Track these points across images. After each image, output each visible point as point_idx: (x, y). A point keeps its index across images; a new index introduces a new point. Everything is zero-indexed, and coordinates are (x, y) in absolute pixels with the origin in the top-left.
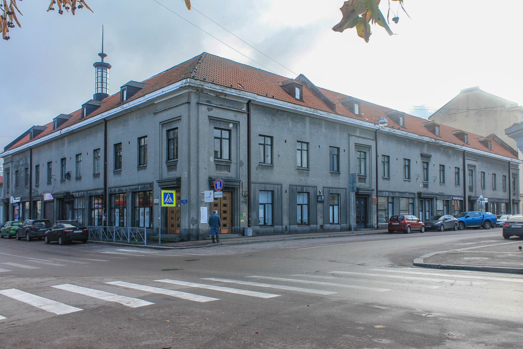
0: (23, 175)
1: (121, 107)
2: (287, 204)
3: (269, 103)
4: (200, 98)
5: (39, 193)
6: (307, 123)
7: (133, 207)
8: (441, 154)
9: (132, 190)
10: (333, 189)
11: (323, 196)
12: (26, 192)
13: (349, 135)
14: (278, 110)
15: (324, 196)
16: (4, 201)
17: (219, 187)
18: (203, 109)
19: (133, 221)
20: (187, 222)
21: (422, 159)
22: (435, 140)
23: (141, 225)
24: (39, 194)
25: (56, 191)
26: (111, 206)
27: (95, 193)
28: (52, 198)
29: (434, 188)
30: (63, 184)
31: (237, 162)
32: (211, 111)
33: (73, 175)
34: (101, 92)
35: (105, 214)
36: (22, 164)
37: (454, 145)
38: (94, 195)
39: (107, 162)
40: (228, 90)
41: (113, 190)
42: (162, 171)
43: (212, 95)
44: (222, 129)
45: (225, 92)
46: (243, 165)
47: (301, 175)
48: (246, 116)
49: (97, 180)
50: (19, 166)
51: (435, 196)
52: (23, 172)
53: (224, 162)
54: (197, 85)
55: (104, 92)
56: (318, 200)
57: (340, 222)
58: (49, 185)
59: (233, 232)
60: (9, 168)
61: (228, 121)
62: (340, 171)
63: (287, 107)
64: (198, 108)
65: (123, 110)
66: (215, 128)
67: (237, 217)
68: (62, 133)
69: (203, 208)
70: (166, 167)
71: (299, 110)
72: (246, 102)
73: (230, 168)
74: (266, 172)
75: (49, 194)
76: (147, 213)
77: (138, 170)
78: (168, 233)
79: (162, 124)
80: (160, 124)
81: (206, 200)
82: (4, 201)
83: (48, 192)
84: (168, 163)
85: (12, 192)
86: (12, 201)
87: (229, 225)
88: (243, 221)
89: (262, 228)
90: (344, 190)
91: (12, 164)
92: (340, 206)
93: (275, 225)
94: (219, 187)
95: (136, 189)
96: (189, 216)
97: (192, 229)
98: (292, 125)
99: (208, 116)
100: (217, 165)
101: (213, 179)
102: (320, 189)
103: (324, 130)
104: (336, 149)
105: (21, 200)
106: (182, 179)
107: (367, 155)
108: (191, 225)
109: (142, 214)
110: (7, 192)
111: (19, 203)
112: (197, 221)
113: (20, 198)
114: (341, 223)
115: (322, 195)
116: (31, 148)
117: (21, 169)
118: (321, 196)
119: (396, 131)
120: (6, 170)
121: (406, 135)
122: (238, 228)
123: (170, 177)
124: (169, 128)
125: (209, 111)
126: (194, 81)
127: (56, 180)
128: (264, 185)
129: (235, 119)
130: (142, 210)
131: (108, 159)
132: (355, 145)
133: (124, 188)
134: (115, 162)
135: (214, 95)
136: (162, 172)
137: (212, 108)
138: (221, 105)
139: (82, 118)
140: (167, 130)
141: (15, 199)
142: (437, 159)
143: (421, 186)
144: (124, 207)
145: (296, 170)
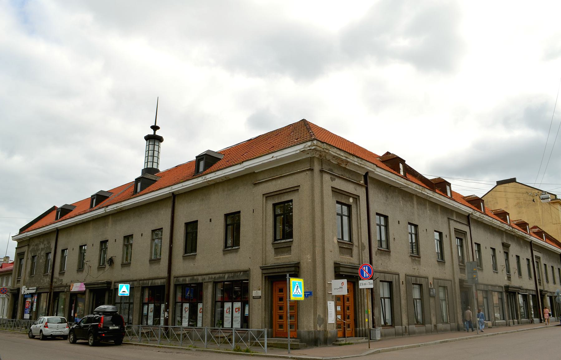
0: (42, 261)
1: (202, 178)
2: (404, 298)
3: (386, 176)
4: (323, 165)
5: (64, 283)
6: (415, 203)
7: (214, 302)
8: (516, 244)
9: (213, 280)
10: (445, 281)
11: (434, 289)
12: (45, 281)
13: (448, 218)
14: (391, 186)
15: (435, 289)
16: (12, 291)
18: (327, 177)
19: (214, 320)
20: (312, 322)
21: (504, 249)
22: (512, 228)
23: (227, 325)
24: (63, 283)
25: (88, 281)
26: (175, 300)
27: (151, 283)
28: (84, 289)
29: (516, 282)
30: (101, 272)
31: (359, 244)
32: (333, 181)
33: (118, 261)
34: (152, 167)
35: (168, 310)
36: (42, 248)
37: (525, 234)
38: (149, 285)
39: (173, 244)
40: (351, 158)
41: (181, 279)
42: (265, 254)
43: (334, 162)
44: (342, 204)
45: (348, 160)
47: (414, 263)
48: (364, 190)
49: (155, 267)
50: (38, 250)
51: (517, 290)
52: (43, 257)
53: (347, 244)
54: (323, 149)
55: (155, 167)
56: (430, 294)
57: (449, 321)
58: (80, 273)
59: (357, 334)
60: (25, 252)
62: (444, 259)
63: (400, 183)
64: (322, 177)
65: (206, 181)
66: (338, 202)
67: (362, 315)
68: (106, 211)
69: (330, 303)
70: (273, 250)
71: (410, 187)
72: (364, 174)
73: (352, 253)
74: (384, 258)
75: (79, 284)
76: (237, 310)
77: (224, 254)
78: (274, 336)
79: (266, 197)
80: (263, 197)
81: (335, 293)
82: (12, 291)
83: (78, 281)
84: (275, 245)
85: (24, 280)
86: (24, 292)
87: (352, 326)
88: (368, 320)
89: (384, 329)
90: (450, 282)
91: (29, 248)
92: (448, 301)
93: (395, 325)
95: (220, 278)
96: (315, 313)
97: (319, 331)
98: (403, 204)
99: (332, 187)
100: (341, 248)
101: (341, 265)
102: (431, 281)
103: (428, 211)
104: (438, 233)
105: (36, 291)
106: (302, 264)
107: (464, 241)
108: (318, 326)
109: (228, 311)
110: (17, 281)
111: (32, 295)
112: (324, 320)
113: (35, 288)
114: (451, 321)
115: (433, 287)
116: (58, 229)
117: (41, 253)
118: (432, 289)
119: (485, 217)
120: (19, 255)
121: (492, 222)
122: (364, 329)
123: (280, 262)
124: (277, 201)
125: (332, 181)
126: (321, 144)
128: (383, 274)
129: (355, 193)
130: (227, 305)
131: (174, 241)
132: (455, 231)
133: (200, 276)
134: (185, 244)
135: (335, 163)
136: (265, 256)
138: (342, 175)
139: (135, 193)
140: (273, 204)
141: (28, 289)
142: (514, 250)
143: (506, 279)
144: (201, 300)
145: (409, 256)
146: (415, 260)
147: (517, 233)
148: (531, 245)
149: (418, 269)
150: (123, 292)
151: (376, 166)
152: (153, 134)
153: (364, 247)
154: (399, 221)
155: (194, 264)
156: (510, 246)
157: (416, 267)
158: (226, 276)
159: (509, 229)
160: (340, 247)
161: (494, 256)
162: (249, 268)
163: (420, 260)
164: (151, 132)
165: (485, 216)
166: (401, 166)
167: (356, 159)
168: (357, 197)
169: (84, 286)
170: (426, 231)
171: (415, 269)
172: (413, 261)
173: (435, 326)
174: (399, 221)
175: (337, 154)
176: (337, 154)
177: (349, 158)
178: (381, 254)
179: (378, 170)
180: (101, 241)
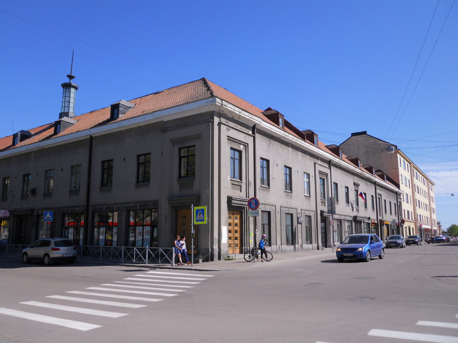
8: (364, 183)
13: (315, 163)
15: (302, 217)
17: (254, 206)
21: (355, 187)
37: (371, 176)
40: (243, 112)
45: (241, 114)
46: (251, 185)
47: (288, 197)
48: (252, 138)
61: (240, 142)
76: (147, 233)
77: (136, 188)
94: (254, 206)
101: (233, 198)
102: (299, 211)
103: (300, 157)
115: (301, 216)
118: (300, 217)
124: (181, 146)
125: (228, 131)
127: (14, 196)
137: (230, 128)
138: (235, 126)
146: (288, 195)
147: (365, 175)
148: (375, 183)
149: (290, 202)
150: (47, 218)
151: (262, 120)
152: (69, 82)
153: (251, 184)
154: (277, 164)
155: (110, 196)
156: (359, 185)
157: (288, 200)
158: (138, 205)
159: (360, 172)
160: (232, 184)
161: (347, 194)
162: (158, 199)
163: (292, 195)
164: (67, 80)
165: (341, 161)
166: (280, 120)
167: (247, 114)
168: (246, 145)
169: (9, 213)
170: (298, 172)
171: (288, 202)
172: (287, 195)
173: (302, 246)
174: (277, 164)
175: (233, 109)
176: (233, 109)
177: (241, 113)
178: (263, 190)
179: (264, 123)
180: (24, 174)
